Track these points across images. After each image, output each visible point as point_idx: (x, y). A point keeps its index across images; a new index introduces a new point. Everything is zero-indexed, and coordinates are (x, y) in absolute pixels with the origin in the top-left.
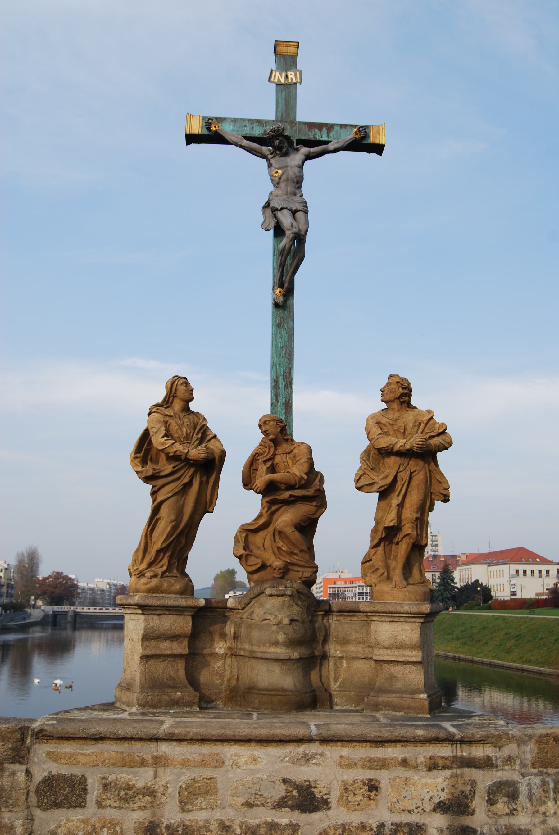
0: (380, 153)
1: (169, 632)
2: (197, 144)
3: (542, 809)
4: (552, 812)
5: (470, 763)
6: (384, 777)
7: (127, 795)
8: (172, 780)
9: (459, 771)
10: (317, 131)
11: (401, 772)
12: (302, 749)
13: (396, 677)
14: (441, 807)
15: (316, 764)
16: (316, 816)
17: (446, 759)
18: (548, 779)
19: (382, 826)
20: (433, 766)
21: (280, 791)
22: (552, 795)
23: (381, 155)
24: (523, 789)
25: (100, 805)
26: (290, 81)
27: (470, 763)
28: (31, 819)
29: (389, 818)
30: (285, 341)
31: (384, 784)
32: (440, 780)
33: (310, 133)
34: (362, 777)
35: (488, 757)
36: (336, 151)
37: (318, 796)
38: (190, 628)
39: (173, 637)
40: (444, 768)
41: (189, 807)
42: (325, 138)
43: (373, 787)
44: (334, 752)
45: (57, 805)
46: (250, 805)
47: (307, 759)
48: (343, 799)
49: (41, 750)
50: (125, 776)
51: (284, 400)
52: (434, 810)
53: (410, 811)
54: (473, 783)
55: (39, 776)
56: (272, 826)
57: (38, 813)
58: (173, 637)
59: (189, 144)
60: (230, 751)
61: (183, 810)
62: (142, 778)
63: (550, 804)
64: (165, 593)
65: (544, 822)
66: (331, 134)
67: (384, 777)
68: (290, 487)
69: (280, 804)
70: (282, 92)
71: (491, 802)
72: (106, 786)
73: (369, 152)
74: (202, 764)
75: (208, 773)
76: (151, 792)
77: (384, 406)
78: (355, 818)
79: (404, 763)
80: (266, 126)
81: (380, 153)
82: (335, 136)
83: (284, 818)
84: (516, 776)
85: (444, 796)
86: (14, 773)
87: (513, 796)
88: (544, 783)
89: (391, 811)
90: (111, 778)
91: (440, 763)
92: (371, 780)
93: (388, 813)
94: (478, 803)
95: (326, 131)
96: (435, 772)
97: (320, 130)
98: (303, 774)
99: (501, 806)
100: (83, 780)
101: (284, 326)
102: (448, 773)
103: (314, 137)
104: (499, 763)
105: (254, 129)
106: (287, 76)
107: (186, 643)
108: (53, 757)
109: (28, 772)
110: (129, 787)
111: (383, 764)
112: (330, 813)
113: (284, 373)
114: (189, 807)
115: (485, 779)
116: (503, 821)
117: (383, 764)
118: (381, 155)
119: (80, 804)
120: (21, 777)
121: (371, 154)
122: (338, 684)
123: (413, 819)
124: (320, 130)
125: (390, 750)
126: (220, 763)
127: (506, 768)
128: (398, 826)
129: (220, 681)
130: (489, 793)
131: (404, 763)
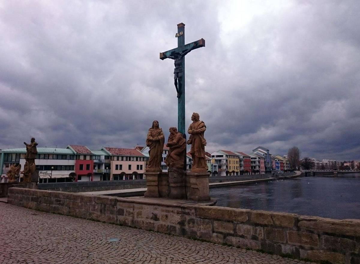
0: (204, 46)
3: (200, 227)
4: (202, 228)
5: (185, 213)
6: (169, 214)
7: (129, 213)
8: (136, 211)
9: (183, 215)
10: (187, 47)
11: (172, 213)
12: (155, 207)
14: (179, 223)
15: (158, 210)
16: (157, 222)
17: (180, 211)
18: (201, 219)
19: (168, 226)
20: (178, 213)
21: (151, 216)
22: (202, 223)
24: (196, 221)
25: (126, 215)
27: (185, 213)
28: (117, 217)
29: (169, 224)
31: (169, 216)
32: (179, 217)
34: (165, 214)
35: (189, 212)
36: (189, 51)
37: (158, 217)
38: (157, 179)
39: (154, 181)
40: (180, 214)
41: (138, 217)
43: (167, 216)
44: (160, 208)
45: (120, 215)
46: (147, 218)
47: (156, 209)
48: (162, 219)
49: (118, 203)
50: (128, 210)
52: (178, 224)
53: (173, 223)
54: (185, 218)
55: (118, 208)
56: (150, 223)
57: (118, 216)
58: (154, 181)
60: (144, 206)
61: (137, 218)
62: (131, 210)
63: (202, 226)
65: (200, 230)
67: (169, 214)
68: (174, 145)
69: (152, 218)
71: (189, 223)
72: (127, 211)
74: (140, 208)
75: (141, 210)
76: (133, 213)
77: (192, 122)
78: (164, 223)
79: (172, 211)
81: (204, 46)
83: (152, 221)
84: (194, 218)
85: (180, 220)
86: (115, 208)
87: (194, 223)
88: (200, 221)
89: (170, 222)
90: (127, 210)
91: (179, 212)
92: (166, 215)
93: (169, 223)
94: (186, 223)
96: (178, 215)
98: (156, 212)
99: (191, 225)
100: (124, 210)
102: (181, 215)
104: (191, 214)
107: (157, 183)
108: (120, 205)
109: (117, 208)
110: (130, 212)
111: (168, 211)
112: (160, 221)
114: (138, 217)
115: (188, 218)
116: (191, 229)
117: (168, 211)
119: (123, 215)
120: (116, 209)
123: (174, 225)
125: (170, 208)
126: (142, 208)
127: (192, 215)
128: (171, 226)
130: (189, 221)
131: (172, 211)
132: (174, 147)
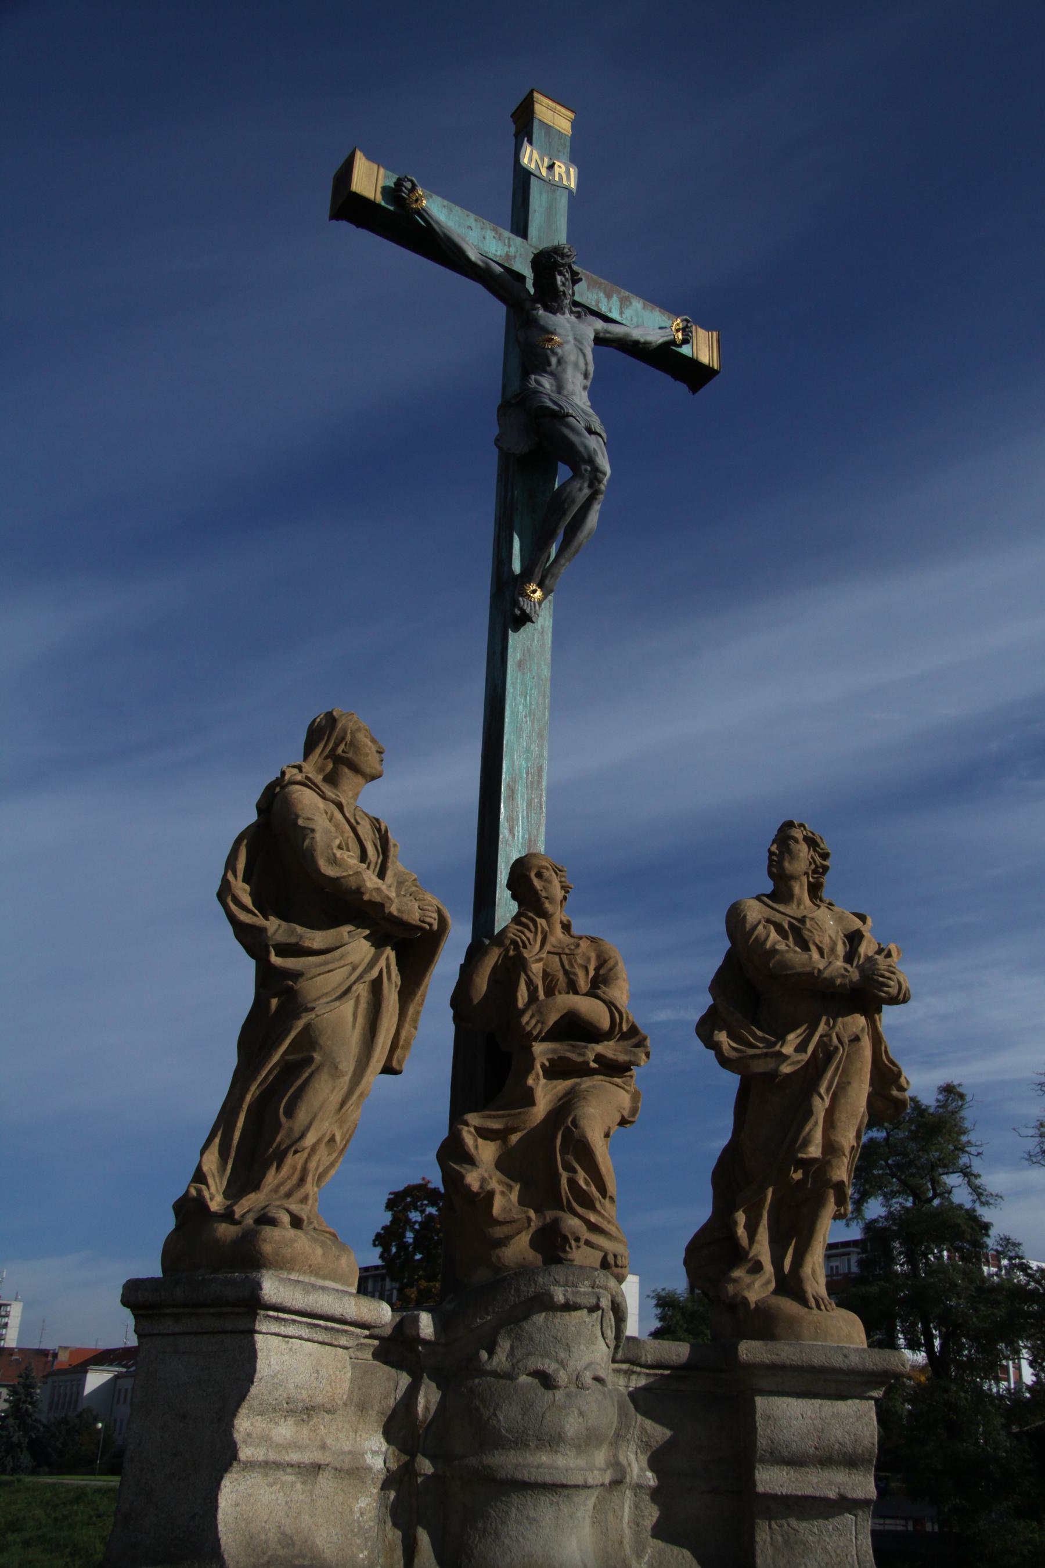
0: (695, 388)
1: (304, 1395)
2: (354, 227)
10: (602, 295)
13: (804, 1543)
23: (694, 393)
26: (557, 179)
30: (531, 704)
33: (590, 295)
42: (614, 315)
51: (526, 836)
59: (337, 220)
64: (317, 1275)
66: (628, 313)
70: (541, 193)
73: (676, 377)
80: (509, 246)
81: (695, 388)
82: (635, 319)
95: (618, 303)
97: (609, 297)
101: (530, 671)
103: (597, 305)
105: (487, 241)
106: (551, 167)
113: (527, 773)
118: (694, 393)
121: (678, 382)
122: (646, 1559)
124: (609, 297)
129: (366, 1553)
132: (599, 1058)
